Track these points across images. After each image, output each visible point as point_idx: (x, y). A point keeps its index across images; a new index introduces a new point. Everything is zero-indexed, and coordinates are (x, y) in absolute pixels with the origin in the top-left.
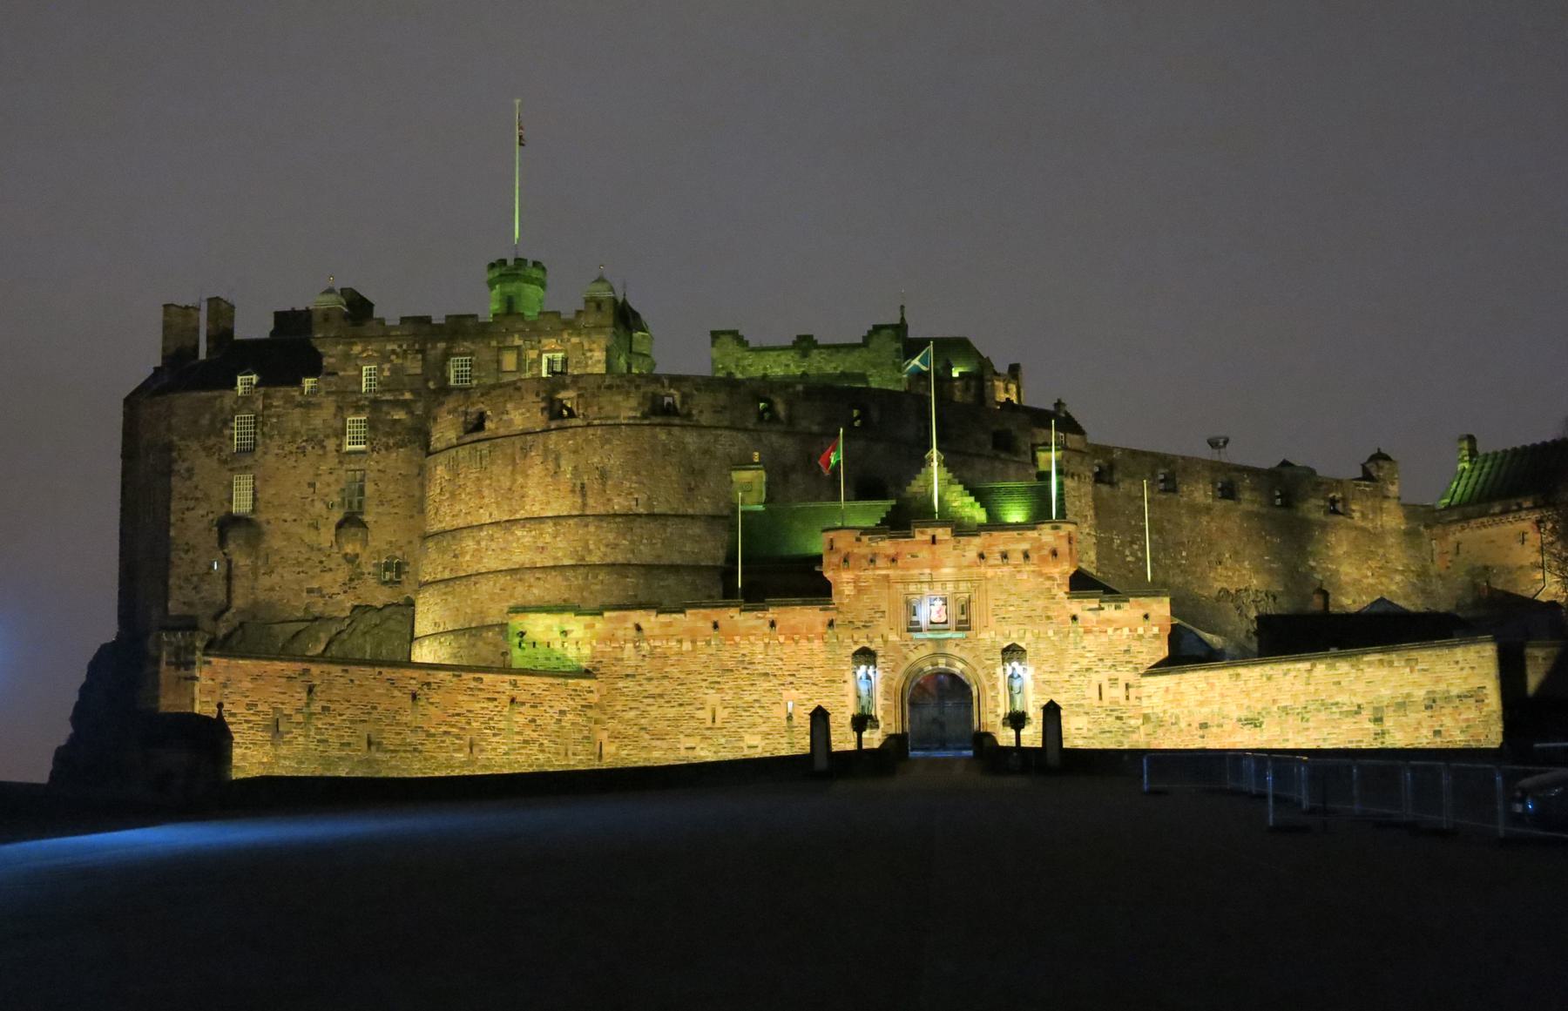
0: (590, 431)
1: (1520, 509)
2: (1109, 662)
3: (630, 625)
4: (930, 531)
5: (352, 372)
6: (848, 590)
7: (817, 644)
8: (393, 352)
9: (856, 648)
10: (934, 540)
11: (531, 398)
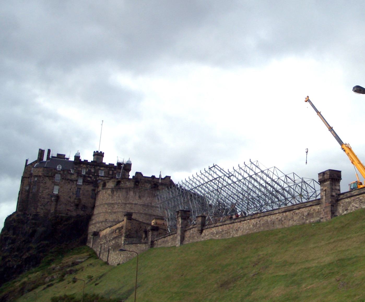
5: (80, 169)
8: (89, 167)
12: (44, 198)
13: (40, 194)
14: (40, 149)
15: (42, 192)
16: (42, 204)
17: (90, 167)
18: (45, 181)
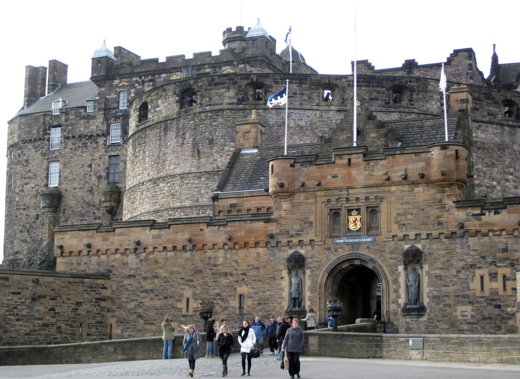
2: (489, 259)
4: (346, 157)
5: (113, 96)
8: (137, 81)
9: (291, 252)
12: (27, 208)
13: (17, 199)
14: (27, 67)
15: (23, 191)
16: (24, 226)
17: (139, 80)
18: (25, 158)
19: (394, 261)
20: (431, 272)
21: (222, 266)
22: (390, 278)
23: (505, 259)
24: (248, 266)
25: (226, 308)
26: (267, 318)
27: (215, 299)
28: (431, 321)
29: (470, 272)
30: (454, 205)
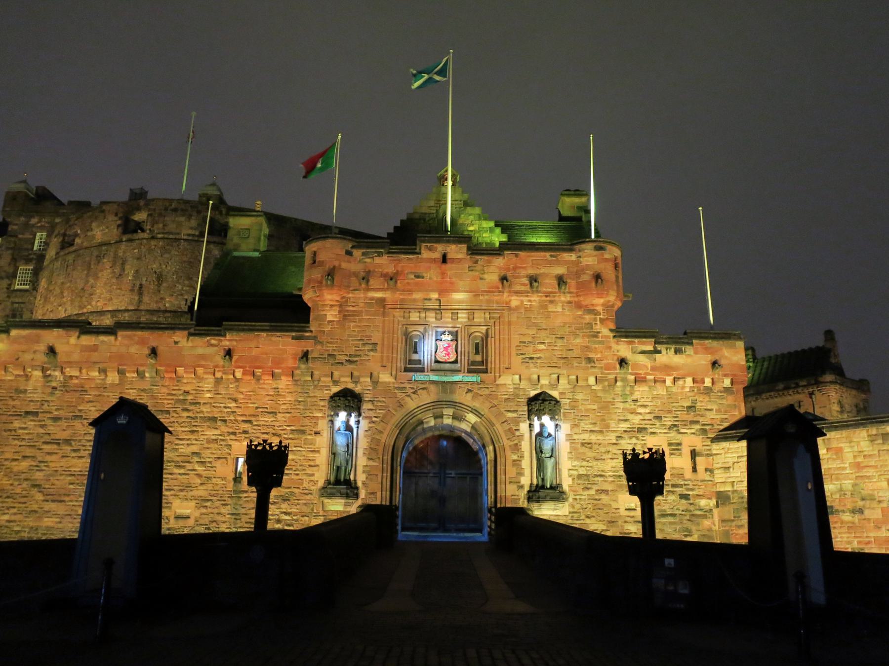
0: (153, 242)
1: (797, 386)
2: (668, 421)
3: (42, 347)
4: (440, 248)
5: (28, 236)
6: (331, 315)
7: (284, 382)
9: (335, 389)
10: (444, 259)
11: (111, 218)
19: (515, 415)
20: (575, 437)
21: (208, 406)
22: (507, 443)
23: (692, 422)
24: (257, 408)
25: (209, 478)
26: (285, 500)
27: (189, 462)
28: (576, 515)
29: (637, 438)
30: (612, 335)
